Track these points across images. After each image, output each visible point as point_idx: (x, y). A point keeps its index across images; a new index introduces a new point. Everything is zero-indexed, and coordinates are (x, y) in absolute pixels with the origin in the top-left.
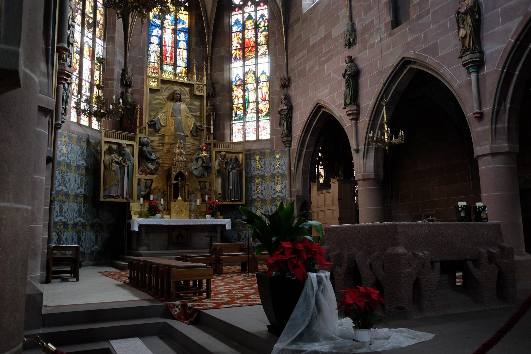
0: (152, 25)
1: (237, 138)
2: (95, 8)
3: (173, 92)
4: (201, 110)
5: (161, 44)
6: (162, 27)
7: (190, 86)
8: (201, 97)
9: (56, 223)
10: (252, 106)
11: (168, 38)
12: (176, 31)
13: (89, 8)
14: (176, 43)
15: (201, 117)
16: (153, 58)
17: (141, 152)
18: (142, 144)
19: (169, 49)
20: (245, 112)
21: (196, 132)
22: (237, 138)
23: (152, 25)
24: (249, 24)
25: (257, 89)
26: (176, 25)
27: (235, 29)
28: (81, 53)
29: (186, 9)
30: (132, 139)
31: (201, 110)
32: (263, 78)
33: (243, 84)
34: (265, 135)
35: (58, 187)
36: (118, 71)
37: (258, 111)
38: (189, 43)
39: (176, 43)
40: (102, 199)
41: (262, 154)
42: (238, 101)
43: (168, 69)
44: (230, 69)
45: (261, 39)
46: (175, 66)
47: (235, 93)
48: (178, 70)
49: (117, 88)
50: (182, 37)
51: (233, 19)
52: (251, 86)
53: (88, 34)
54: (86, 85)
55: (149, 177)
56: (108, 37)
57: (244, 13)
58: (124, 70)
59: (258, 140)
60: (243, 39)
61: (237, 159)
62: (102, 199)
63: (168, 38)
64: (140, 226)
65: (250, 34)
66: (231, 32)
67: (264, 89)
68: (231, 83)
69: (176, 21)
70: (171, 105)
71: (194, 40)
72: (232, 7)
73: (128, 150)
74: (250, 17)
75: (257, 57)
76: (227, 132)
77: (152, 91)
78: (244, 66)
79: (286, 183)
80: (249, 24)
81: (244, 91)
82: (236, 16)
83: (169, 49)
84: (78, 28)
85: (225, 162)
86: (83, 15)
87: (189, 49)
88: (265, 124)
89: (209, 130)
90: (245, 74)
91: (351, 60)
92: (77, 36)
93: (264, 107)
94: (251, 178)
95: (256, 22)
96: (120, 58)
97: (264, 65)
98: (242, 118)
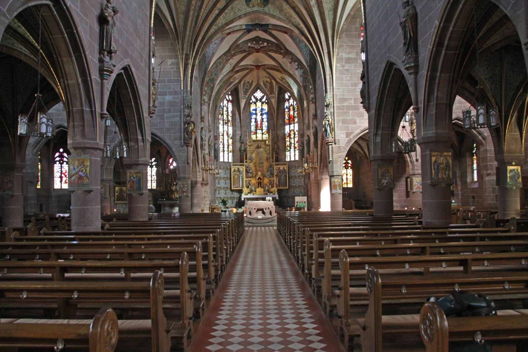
0: (251, 114)
1: (288, 159)
2: (228, 116)
3: (258, 144)
4: (269, 150)
5: (256, 121)
6: (256, 114)
7: (265, 141)
8: (268, 145)
9: (217, 198)
10: (293, 145)
11: (259, 118)
12: (262, 115)
13: (225, 117)
14: (262, 119)
15: (269, 153)
16: (253, 128)
17: (246, 170)
18: (247, 167)
19: (259, 123)
20: (290, 148)
21: (267, 159)
22: (288, 159)
23: (251, 114)
24: (291, 108)
25: (294, 137)
26: (262, 112)
27: (286, 110)
28: (223, 135)
29: (266, 103)
30: (243, 165)
31: (269, 150)
32: (297, 133)
33: (290, 135)
34: (297, 159)
35: (217, 185)
36: (238, 138)
37: (295, 148)
38: (268, 118)
39: (262, 119)
40: (232, 189)
41: (295, 167)
42: (288, 143)
43: (259, 132)
44: (284, 129)
45: (296, 115)
46: (262, 130)
47: (287, 139)
48: (264, 131)
49: (238, 145)
50: (265, 116)
51: (286, 106)
52: (292, 136)
53: (226, 127)
54: (226, 146)
55: (250, 179)
56: (234, 125)
57: (289, 103)
58: (241, 137)
59: (295, 161)
60: (289, 114)
61: (284, 170)
62: (232, 189)
63: (259, 118)
64: (244, 198)
65: (292, 113)
66: (285, 112)
67: (296, 139)
68: (285, 135)
69: (262, 109)
70: (258, 150)
71: (269, 117)
72: (285, 100)
73: (241, 169)
74: (291, 105)
75: (294, 123)
76: (283, 157)
77: (249, 145)
78: (290, 127)
79: (303, 179)
80: (291, 108)
81: (290, 138)
82: (287, 104)
83: (259, 123)
84: (221, 127)
85: (280, 171)
86: (223, 121)
87: (268, 121)
88: (297, 152)
89: (273, 158)
90: (290, 131)
91: (308, 135)
92: (221, 130)
93: (296, 145)
94: (292, 177)
95: (293, 107)
96: (239, 132)
97: (296, 127)
98: (290, 151)
